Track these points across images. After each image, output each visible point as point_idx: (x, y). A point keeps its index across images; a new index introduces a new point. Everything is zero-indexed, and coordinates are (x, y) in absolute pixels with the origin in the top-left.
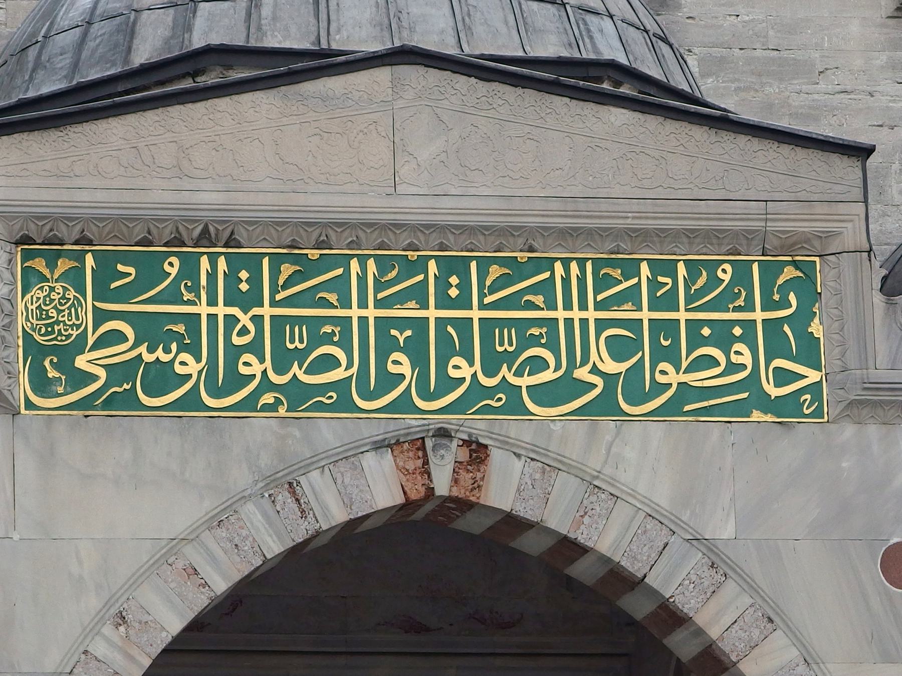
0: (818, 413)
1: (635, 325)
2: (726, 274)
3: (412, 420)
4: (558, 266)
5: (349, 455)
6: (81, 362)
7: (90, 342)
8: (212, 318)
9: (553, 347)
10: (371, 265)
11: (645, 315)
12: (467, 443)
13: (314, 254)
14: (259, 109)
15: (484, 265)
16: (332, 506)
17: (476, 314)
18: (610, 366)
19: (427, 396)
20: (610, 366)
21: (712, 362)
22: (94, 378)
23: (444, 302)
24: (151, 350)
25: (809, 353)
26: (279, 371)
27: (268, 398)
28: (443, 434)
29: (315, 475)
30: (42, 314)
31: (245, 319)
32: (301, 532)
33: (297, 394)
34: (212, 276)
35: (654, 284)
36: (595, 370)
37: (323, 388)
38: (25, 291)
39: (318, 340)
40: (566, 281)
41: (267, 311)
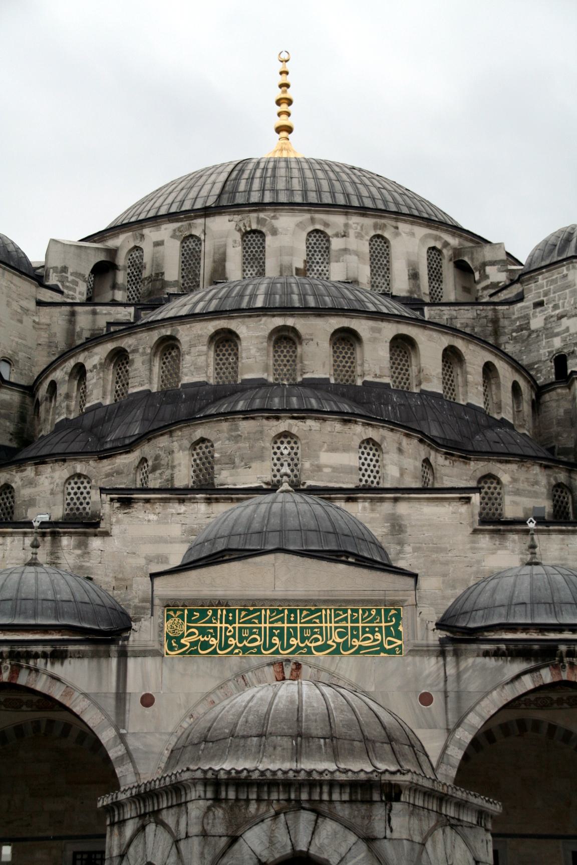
0: (401, 653)
1: (346, 628)
2: (374, 612)
4: (324, 611)
6: (182, 641)
8: (221, 628)
9: (321, 634)
10: (268, 612)
11: (349, 625)
12: (295, 663)
13: (251, 608)
14: (235, 567)
15: (301, 611)
17: (298, 625)
18: (339, 640)
19: (283, 649)
20: (339, 640)
21: (369, 639)
22: (186, 646)
23: (289, 622)
25: (398, 636)
26: (240, 642)
27: (237, 651)
28: (288, 661)
29: (250, 673)
30: (172, 627)
31: (230, 628)
33: (245, 649)
34: (221, 616)
35: (352, 616)
36: (334, 641)
37: (252, 648)
39: (251, 633)
40: (326, 615)
41: (237, 625)
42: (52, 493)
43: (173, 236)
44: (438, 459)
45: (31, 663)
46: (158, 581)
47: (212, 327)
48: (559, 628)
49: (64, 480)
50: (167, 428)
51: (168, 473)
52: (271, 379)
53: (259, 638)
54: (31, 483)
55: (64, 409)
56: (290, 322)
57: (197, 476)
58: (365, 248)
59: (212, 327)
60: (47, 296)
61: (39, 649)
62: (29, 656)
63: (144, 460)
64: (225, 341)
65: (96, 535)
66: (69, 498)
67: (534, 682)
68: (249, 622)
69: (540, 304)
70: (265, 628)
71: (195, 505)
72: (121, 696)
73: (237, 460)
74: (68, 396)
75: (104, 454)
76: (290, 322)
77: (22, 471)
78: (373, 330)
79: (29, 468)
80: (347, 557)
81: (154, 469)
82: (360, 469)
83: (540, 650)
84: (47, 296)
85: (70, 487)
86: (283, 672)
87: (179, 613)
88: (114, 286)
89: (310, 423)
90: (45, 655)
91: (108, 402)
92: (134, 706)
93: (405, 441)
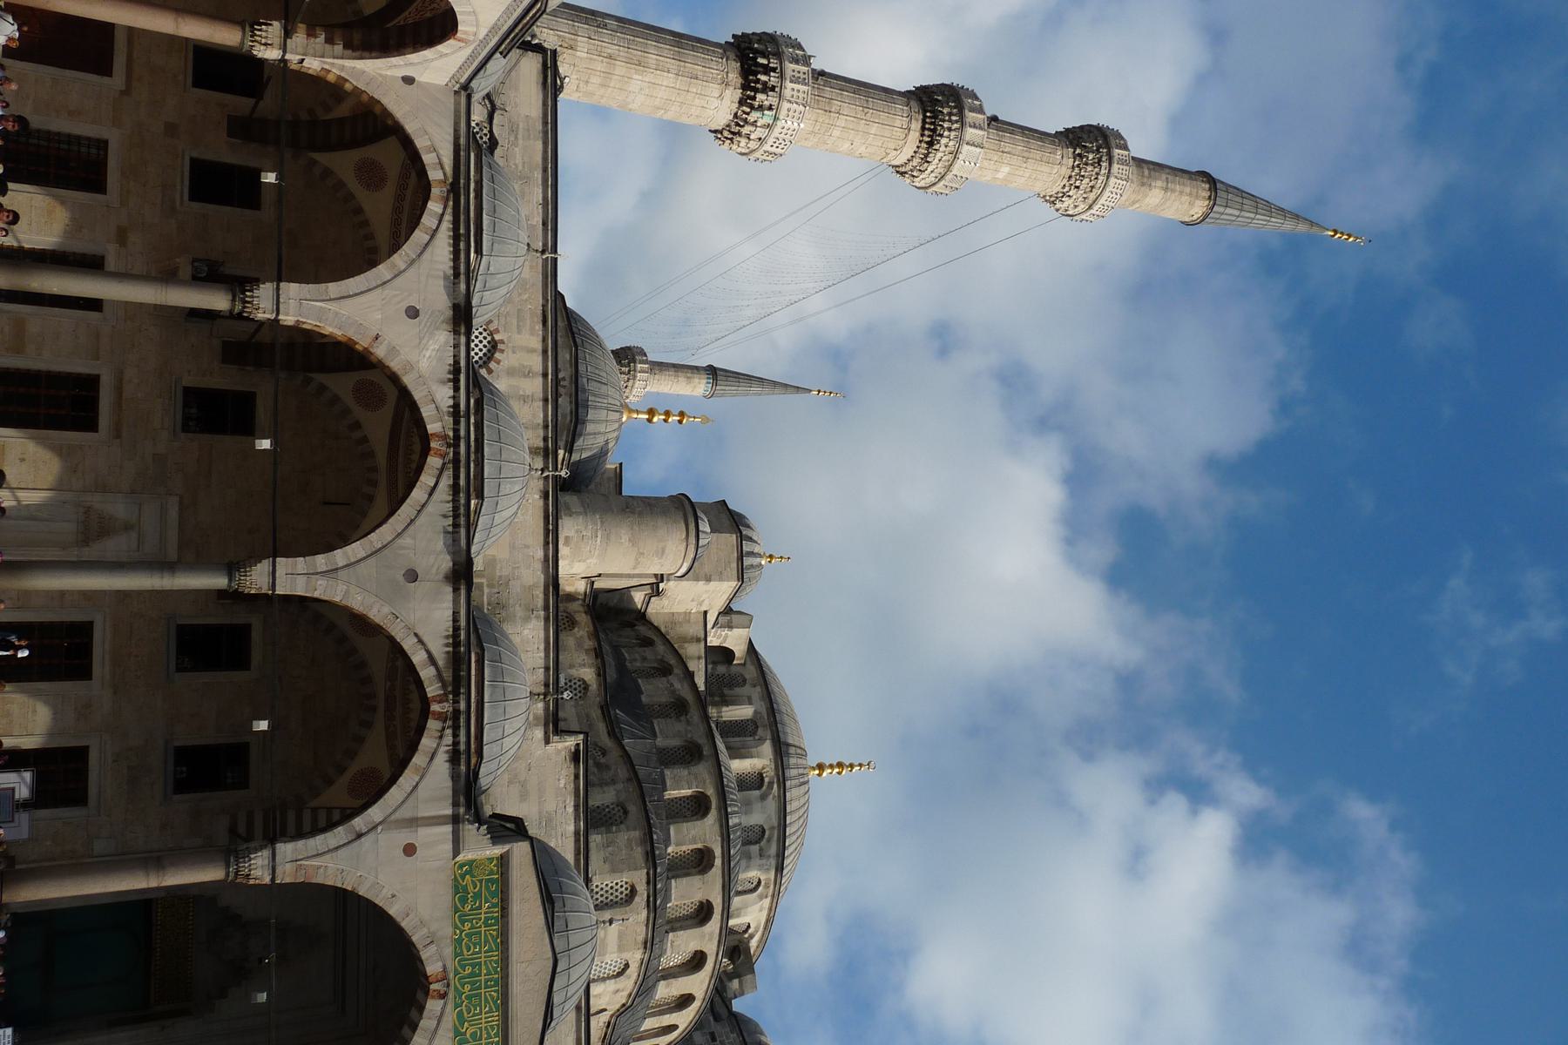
5: (441, 958)
32: (419, 947)
43: (756, 712)
44: (604, 1017)
45: (449, 732)
47: (710, 792)
50: (635, 777)
52: (670, 850)
54: (579, 645)
55: (636, 659)
56: (718, 862)
58: (753, 874)
59: (710, 792)
60: (711, 619)
61: (463, 739)
62: (456, 728)
64: (697, 807)
69: (714, 1039)
72: (414, 822)
74: (644, 659)
75: (605, 709)
76: (718, 862)
78: (711, 934)
81: (598, 765)
84: (711, 619)
88: (714, 663)
89: (645, 913)
90: (456, 743)
91: (643, 699)
92: (404, 837)
93: (626, 993)
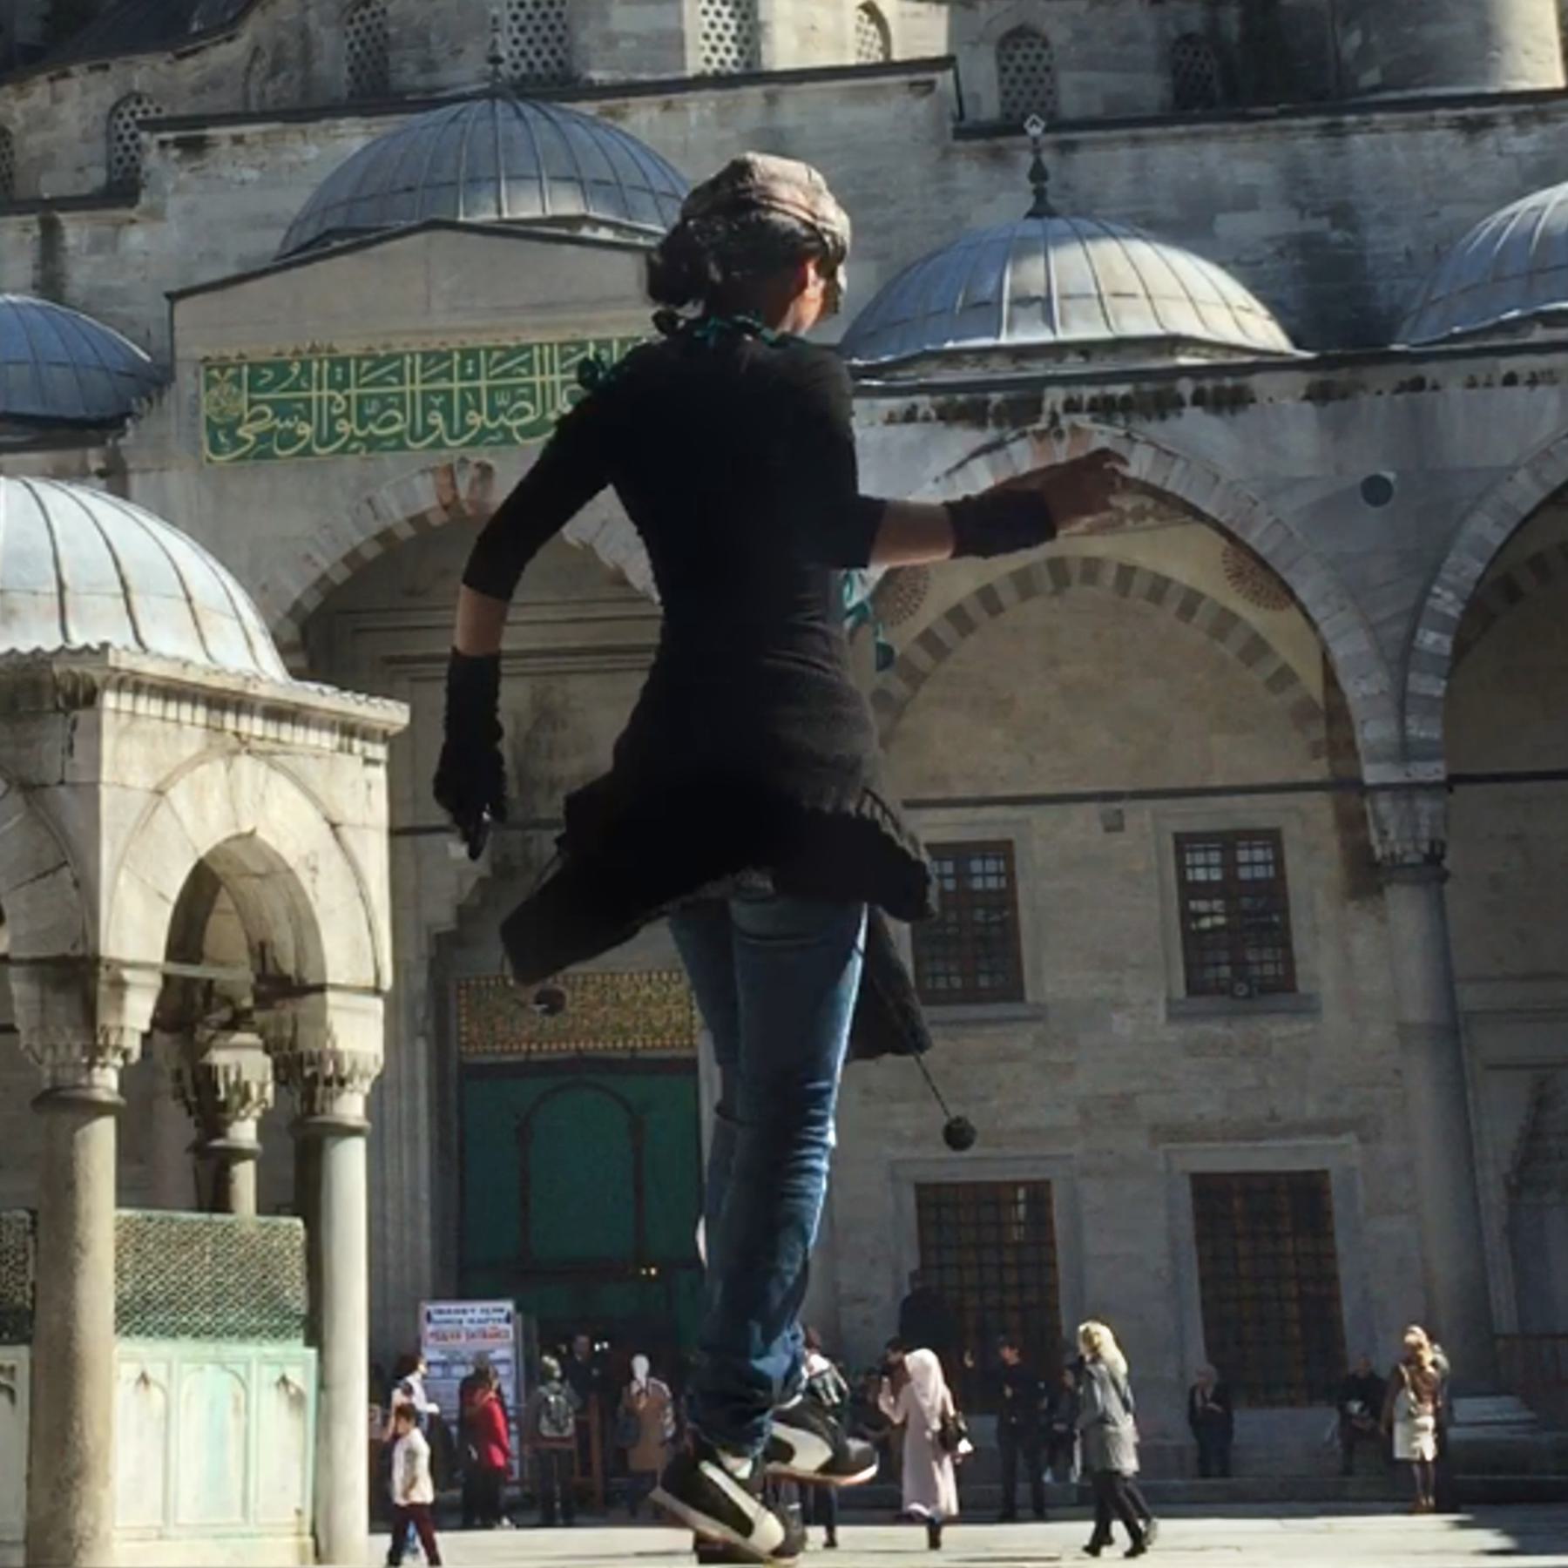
3: (444, 453)
4: (536, 351)
6: (241, 432)
7: (246, 416)
8: (320, 399)
16: (395, 512)
17: (483, 383)
19: (452, 437)
22: (246, 441)
23: (463, 378)
24: (283, 420)
27: (354, 446)
31: (339, 398)
33: (372, 443)
38: (208, 388)
39: (386, 406)
41: (353, 391)
42: (86, 138)
46: (182, 306)
48: (1058, 350)
49: (106, 110)
51: (298, 75)
53: (398, 415)
54: (43, 120)
57: (357, 80)
63: (256, 52)
65: (133, 222)
66: (119, 146)
67: (994, 469)
68: (379, 382)
70: (413, 394)
71: (339, 142)
73: (433, 37)
77: (27, 96)
79: (38, 90)
80: (595, 229)
82: (707, 37)
83: (1006, 401)
85: (121, 123)
86: (453, 485)
87: (230, 372)
